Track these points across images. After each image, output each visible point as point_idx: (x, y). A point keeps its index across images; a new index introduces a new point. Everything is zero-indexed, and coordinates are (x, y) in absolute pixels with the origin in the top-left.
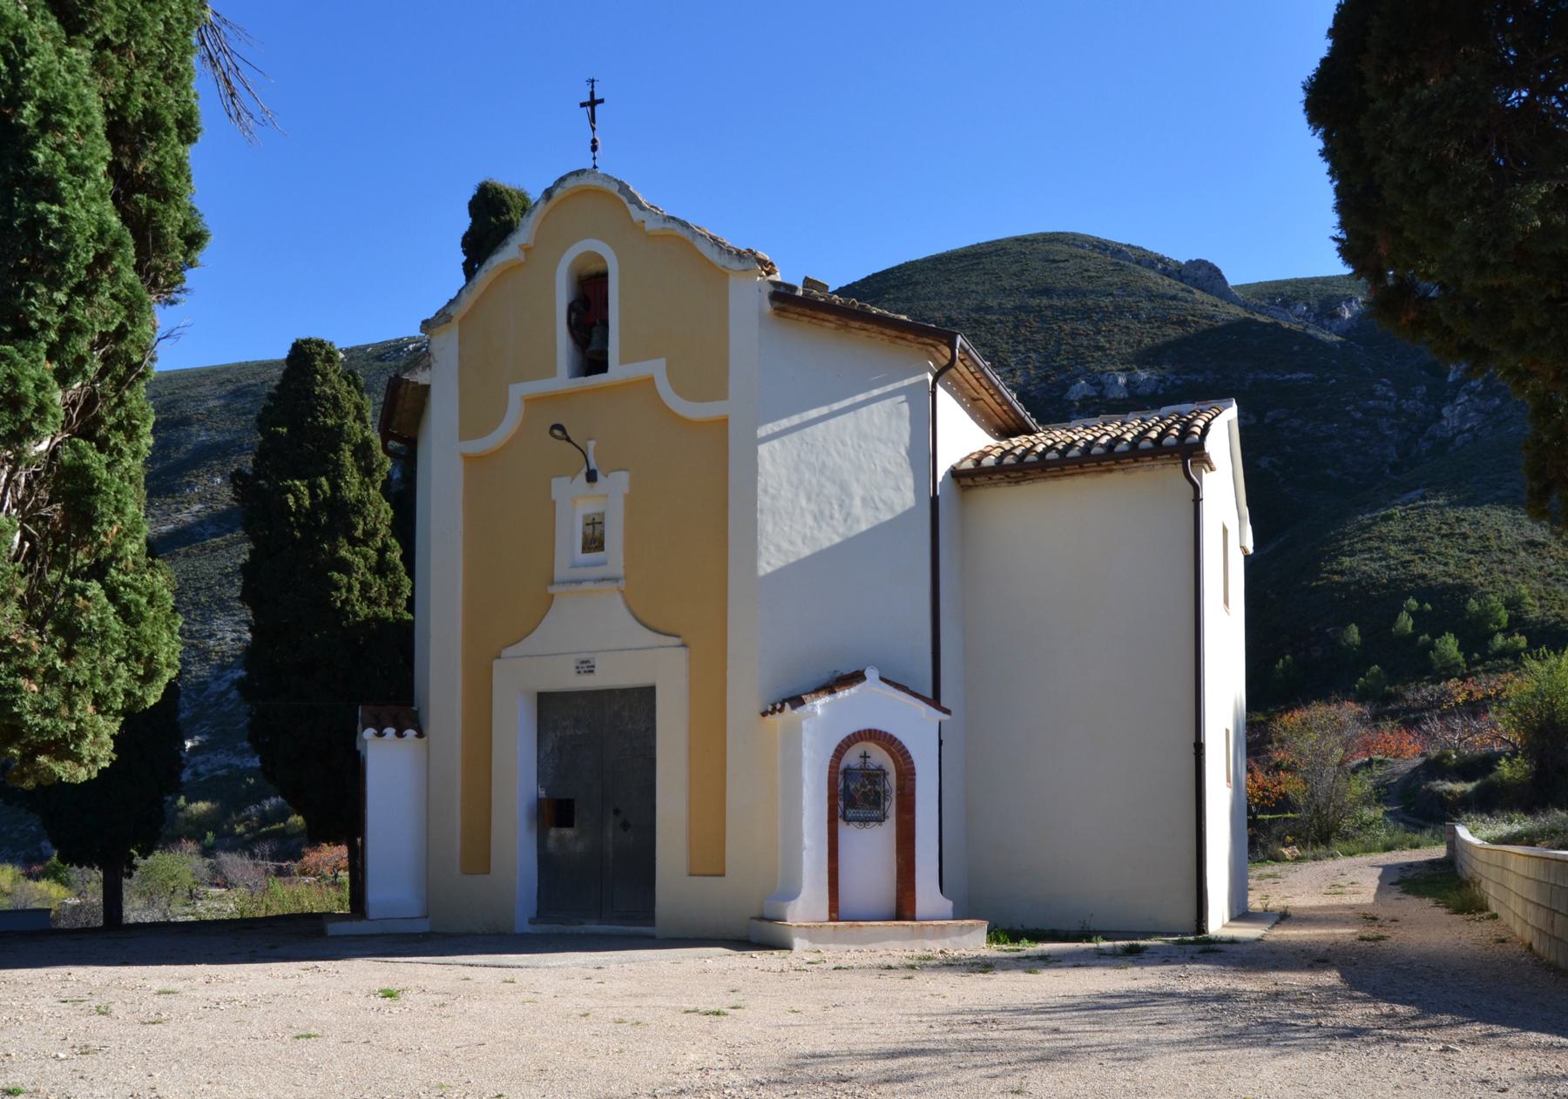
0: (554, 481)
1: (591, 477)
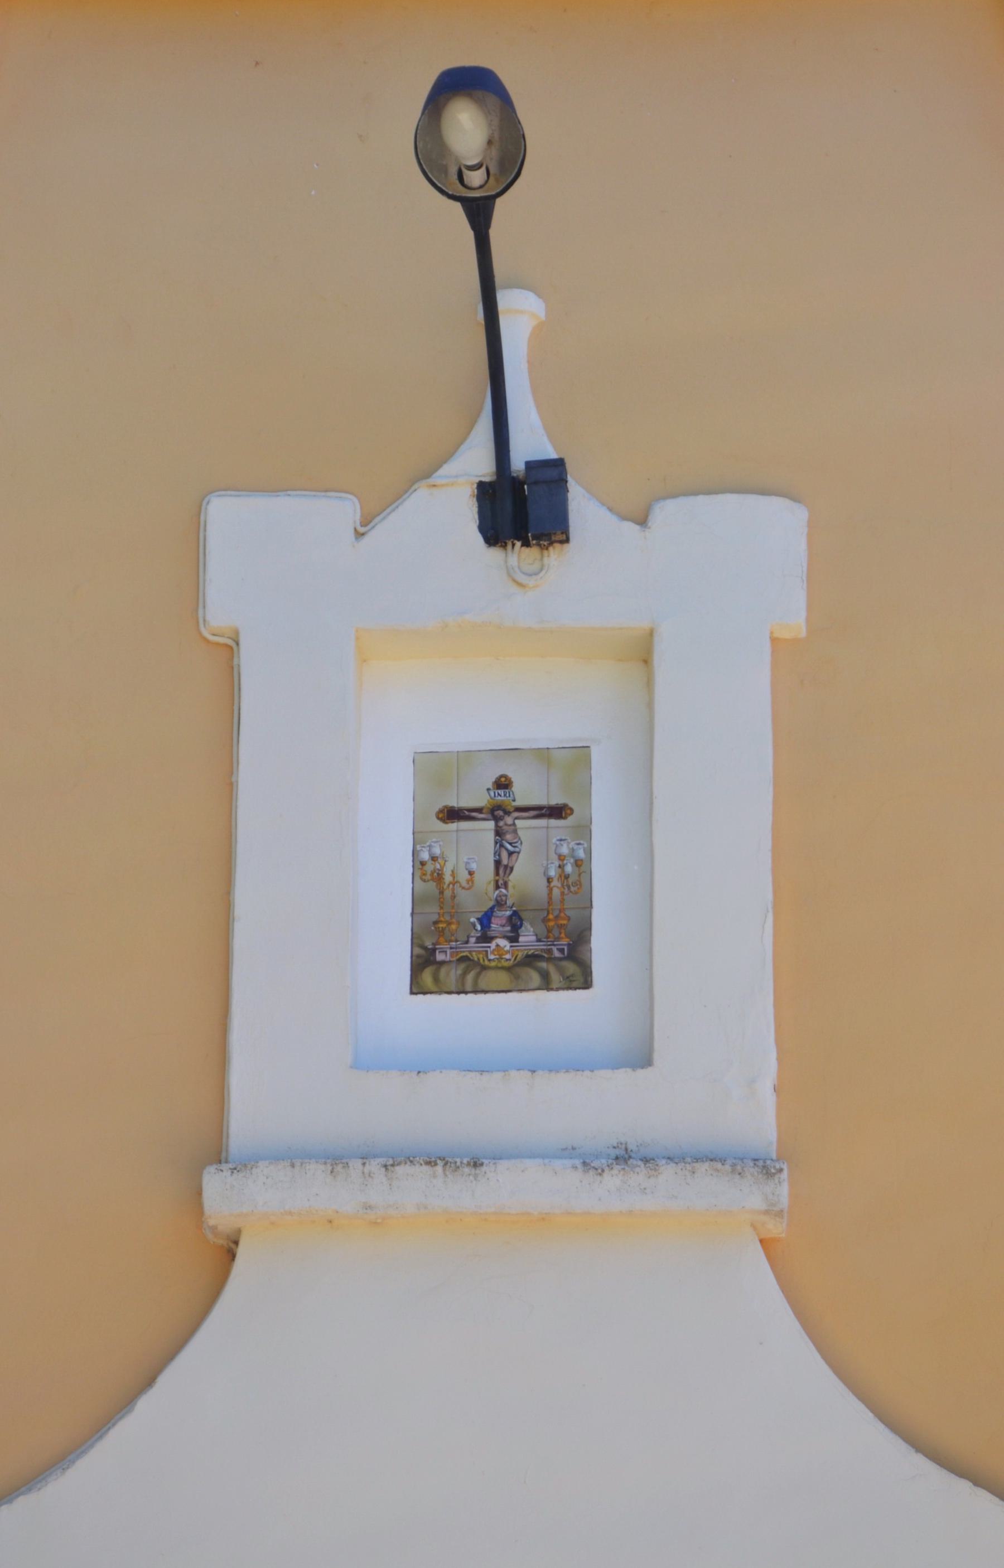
0: (221, 511)
1: (521, 509)
